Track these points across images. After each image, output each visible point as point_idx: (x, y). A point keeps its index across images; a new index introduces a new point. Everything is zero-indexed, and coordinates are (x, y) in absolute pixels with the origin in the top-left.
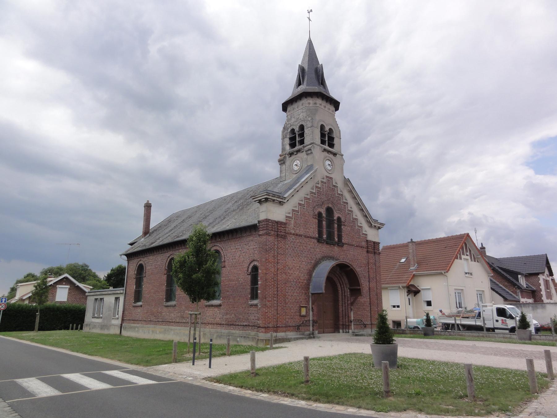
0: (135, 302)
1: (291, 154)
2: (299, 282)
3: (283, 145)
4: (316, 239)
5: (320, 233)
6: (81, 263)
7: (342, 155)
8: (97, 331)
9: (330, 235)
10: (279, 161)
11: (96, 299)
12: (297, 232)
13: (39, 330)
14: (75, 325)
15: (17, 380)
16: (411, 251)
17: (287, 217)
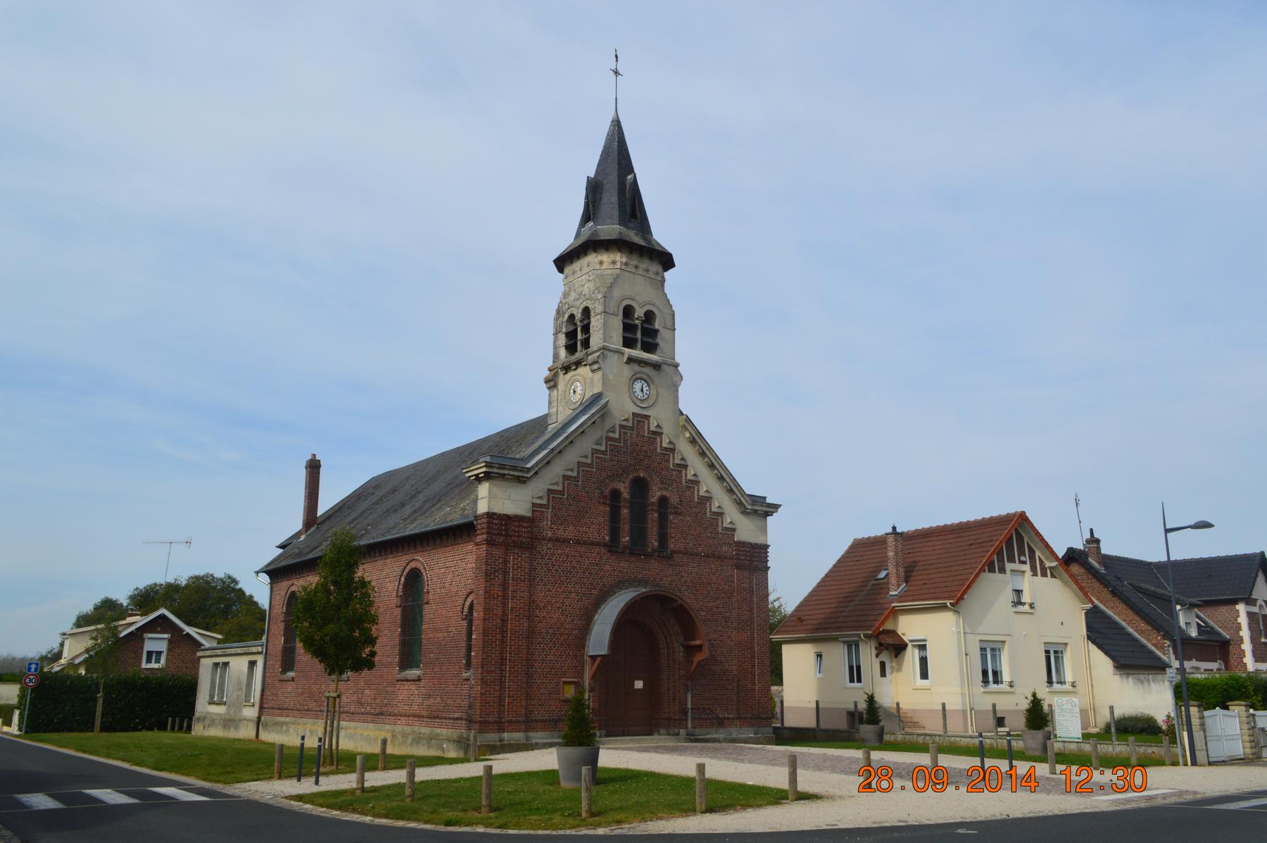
0: (284, 671)
1: (566, 369)
2: (561, 634)
3: (555, 347)
4: (605, 545)
5: (615, 533)
6: (219, 574)
7: (676, 366)
8: (216, 732)
9: (639, 535)
10: (547, 381)
11: (216, 665)
12: (560, 533)
13: (105, 728)
14: (182, 721)
15: (20, 796)
16: (891, 554)
17: (534, 505)
